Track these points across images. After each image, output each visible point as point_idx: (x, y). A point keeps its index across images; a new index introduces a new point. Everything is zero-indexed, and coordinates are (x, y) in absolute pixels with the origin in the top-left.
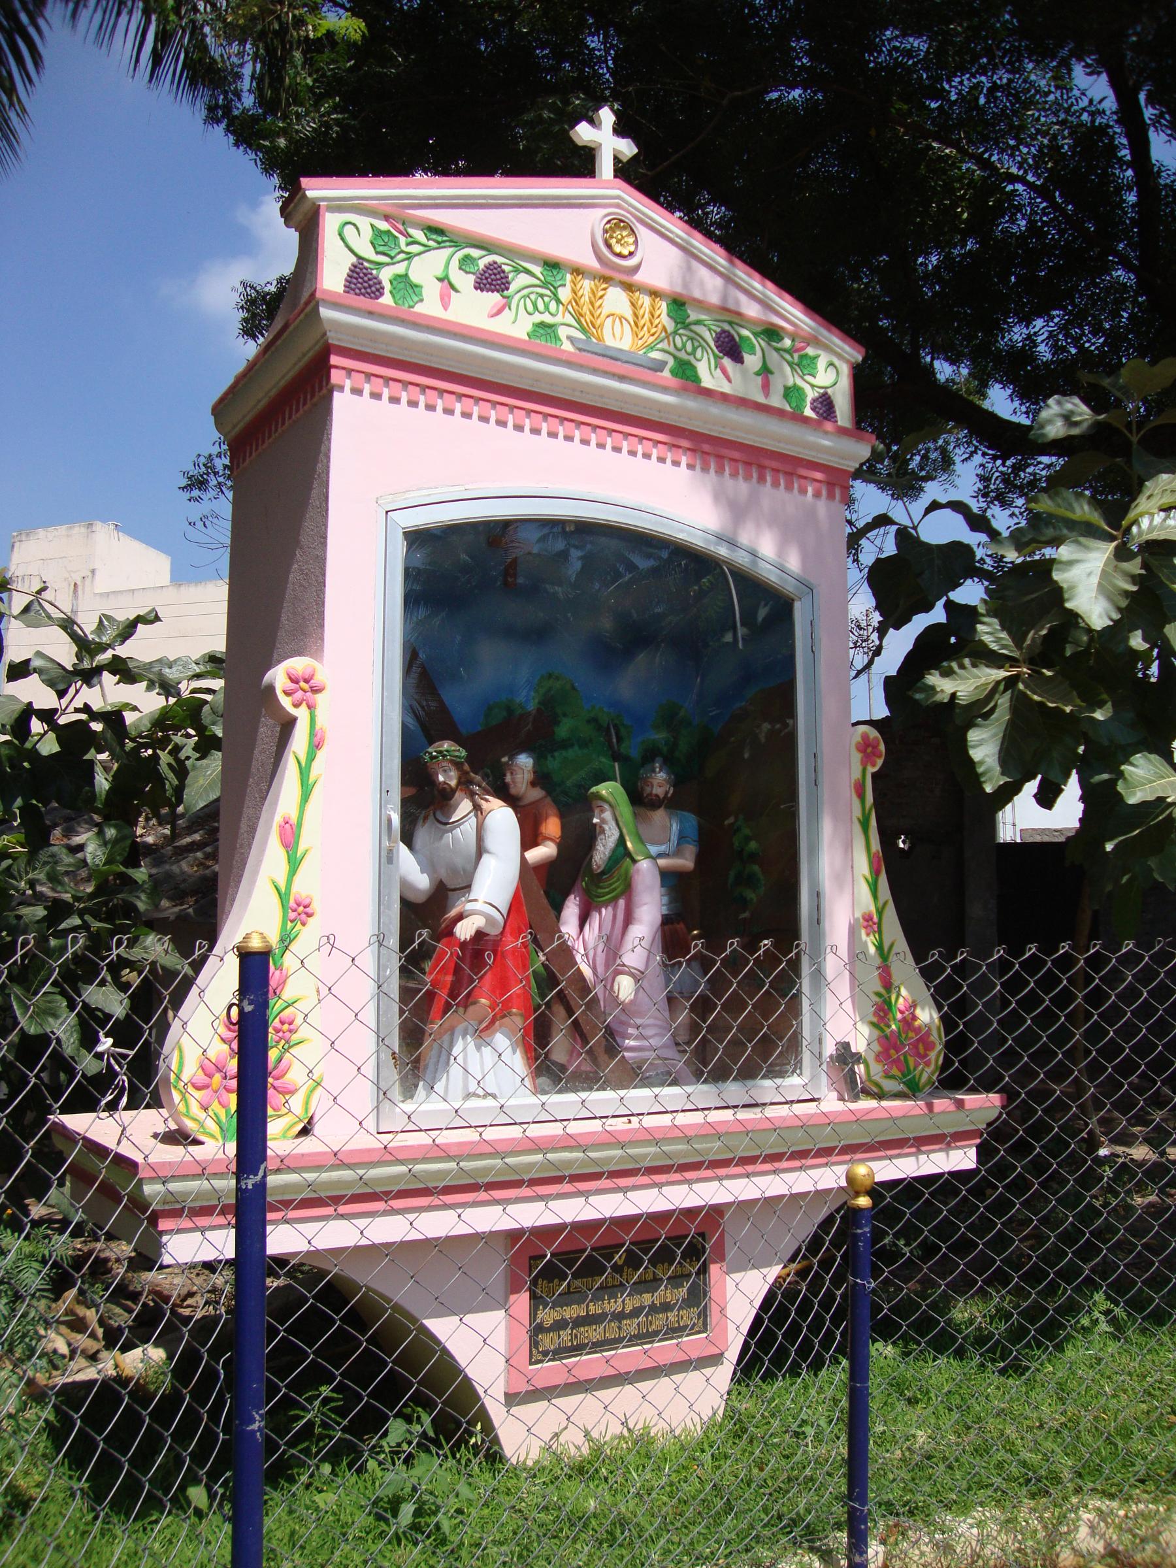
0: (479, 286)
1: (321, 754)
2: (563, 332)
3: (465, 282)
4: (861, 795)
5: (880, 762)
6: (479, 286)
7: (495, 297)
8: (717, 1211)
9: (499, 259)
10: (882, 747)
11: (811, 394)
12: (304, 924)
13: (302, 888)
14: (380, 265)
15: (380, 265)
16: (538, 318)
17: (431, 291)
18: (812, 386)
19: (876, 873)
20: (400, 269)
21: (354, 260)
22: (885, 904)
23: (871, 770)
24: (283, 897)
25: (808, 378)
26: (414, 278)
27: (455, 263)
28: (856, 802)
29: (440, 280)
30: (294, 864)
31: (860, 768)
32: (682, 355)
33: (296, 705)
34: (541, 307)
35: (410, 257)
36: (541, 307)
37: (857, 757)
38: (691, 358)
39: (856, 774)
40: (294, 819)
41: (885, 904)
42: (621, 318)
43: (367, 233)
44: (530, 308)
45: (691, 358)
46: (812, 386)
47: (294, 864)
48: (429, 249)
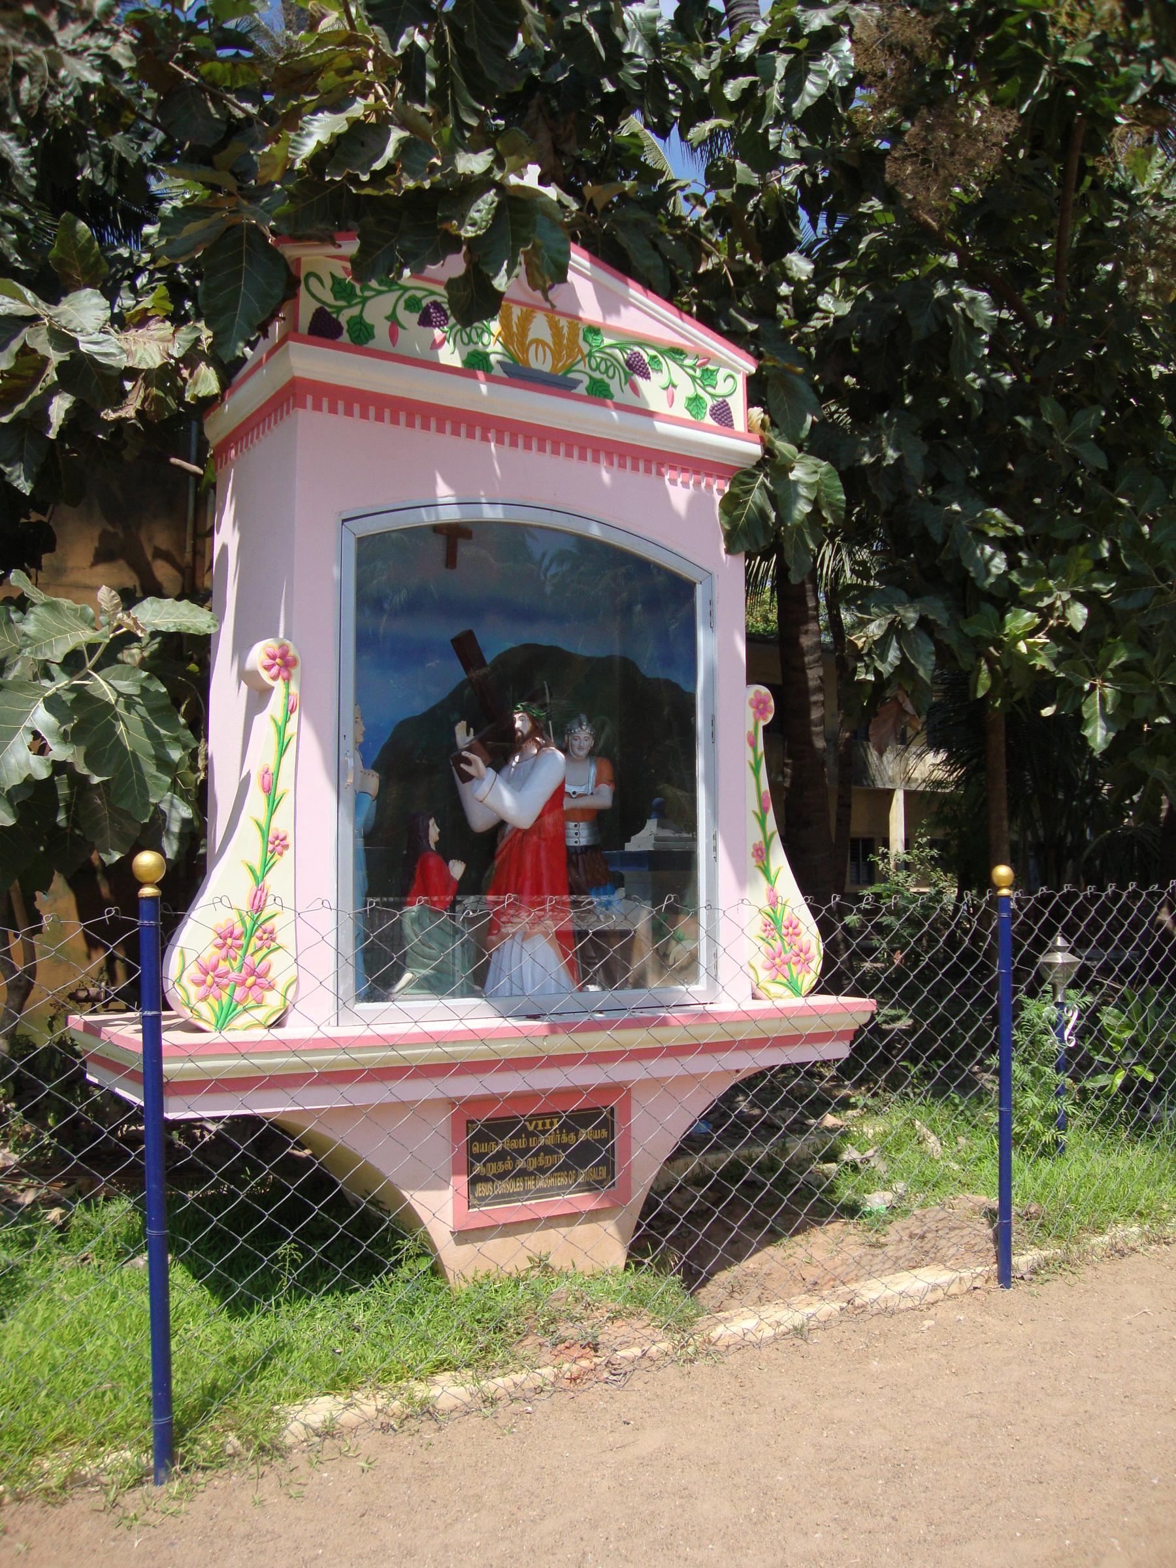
3: (410, 319)
4: (753, 744)
5: (770, 717)
10: (772, 703)
11: (710, 402)
12: (281, 854)
13: (282, 823)
14: (339, 310)
17: (381, 329)
18: (712, 396)
19: (764, 810)
20: (355, 311)
21: (319, 305)
22: (772, 835)
23: (762, 723)
24: (264, 832)
25: (709, 389)
26: (368, 319)
27: (401, 304)
28: (749, 750)
29: (387, 318)
32: (597, 375)
33: (274, 678)
35: (365, 300)
37: (750, 711)
38: (604, 377)
39: (750, 728)
40: (272, 769)
41: (772, 835)
42: (544, 344)
43: (328, 282)
44: (466, 340)
45: (604, 377)
46: (712, 396)
48: (380, 293)
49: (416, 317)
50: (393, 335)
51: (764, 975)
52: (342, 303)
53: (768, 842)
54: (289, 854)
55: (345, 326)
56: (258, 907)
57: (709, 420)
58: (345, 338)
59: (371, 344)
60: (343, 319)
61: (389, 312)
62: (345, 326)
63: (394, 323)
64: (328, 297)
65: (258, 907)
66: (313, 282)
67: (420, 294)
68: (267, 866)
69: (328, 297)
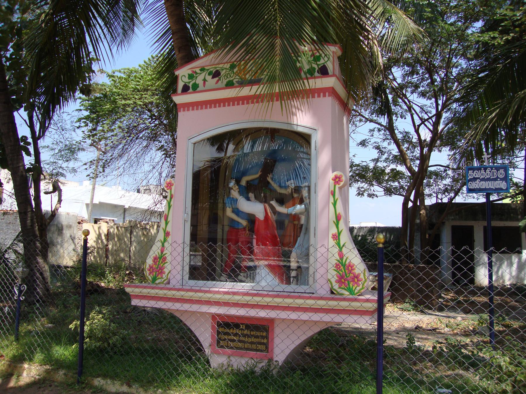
0: (213, 78)
1: (173, 200)
2: (234, 81)
3: (209, 78)
6: (213, 78)
7: (217, 79)
8: (271, 321)
9: (218, 69)
13: (169, 229)
14: (189, 82)
15: (189, 82)
16: (228, 79)
18: (318, 65)
20: (194, 82)
24: (165, 231)
26: (197, 83)
30: (167, 224)
31: (333, 185)
34: (229, 77)
36: (229, 77)
43: (187, 76)
47: (167, 224)
48: (201, 74)
49: (211, 76)
50: (204, 86)
51: (336, 286)
52: (191, 80)
53: (339, 233)
54: (170, 237)
55: (191, 86)
56: (162, 251)
57: (316, 74)
58: (191, 90)
59: (198, 89)
60: (190, 85)
61: (203, 78)
62: (191, 86)
63: (205, 81)
64: (186, 80)
65: (162, 251)
66: (184, 77)
67: (212, 70)
68: (165, 240)
69: (186, 80)
